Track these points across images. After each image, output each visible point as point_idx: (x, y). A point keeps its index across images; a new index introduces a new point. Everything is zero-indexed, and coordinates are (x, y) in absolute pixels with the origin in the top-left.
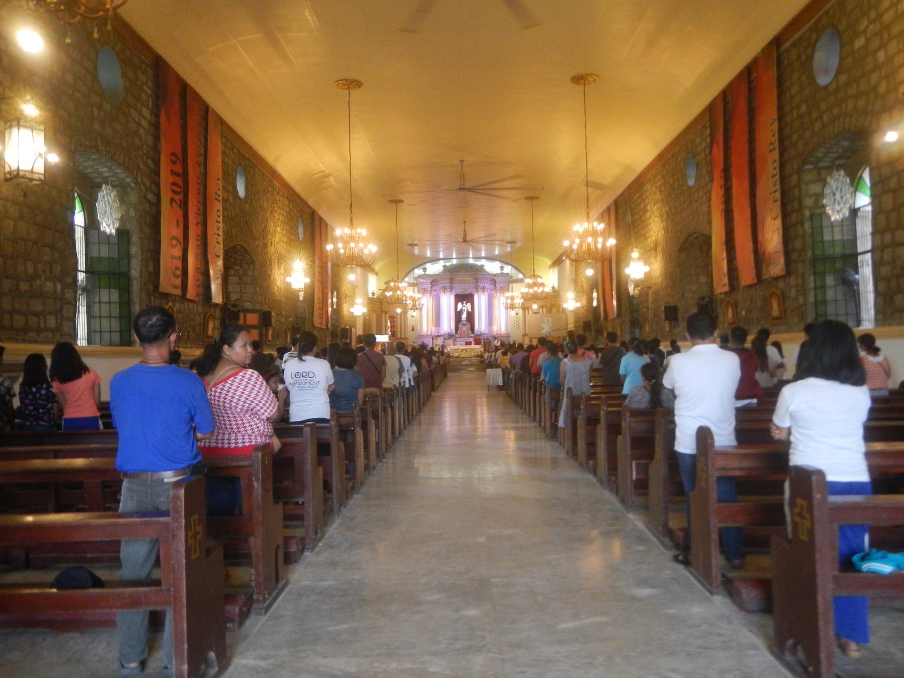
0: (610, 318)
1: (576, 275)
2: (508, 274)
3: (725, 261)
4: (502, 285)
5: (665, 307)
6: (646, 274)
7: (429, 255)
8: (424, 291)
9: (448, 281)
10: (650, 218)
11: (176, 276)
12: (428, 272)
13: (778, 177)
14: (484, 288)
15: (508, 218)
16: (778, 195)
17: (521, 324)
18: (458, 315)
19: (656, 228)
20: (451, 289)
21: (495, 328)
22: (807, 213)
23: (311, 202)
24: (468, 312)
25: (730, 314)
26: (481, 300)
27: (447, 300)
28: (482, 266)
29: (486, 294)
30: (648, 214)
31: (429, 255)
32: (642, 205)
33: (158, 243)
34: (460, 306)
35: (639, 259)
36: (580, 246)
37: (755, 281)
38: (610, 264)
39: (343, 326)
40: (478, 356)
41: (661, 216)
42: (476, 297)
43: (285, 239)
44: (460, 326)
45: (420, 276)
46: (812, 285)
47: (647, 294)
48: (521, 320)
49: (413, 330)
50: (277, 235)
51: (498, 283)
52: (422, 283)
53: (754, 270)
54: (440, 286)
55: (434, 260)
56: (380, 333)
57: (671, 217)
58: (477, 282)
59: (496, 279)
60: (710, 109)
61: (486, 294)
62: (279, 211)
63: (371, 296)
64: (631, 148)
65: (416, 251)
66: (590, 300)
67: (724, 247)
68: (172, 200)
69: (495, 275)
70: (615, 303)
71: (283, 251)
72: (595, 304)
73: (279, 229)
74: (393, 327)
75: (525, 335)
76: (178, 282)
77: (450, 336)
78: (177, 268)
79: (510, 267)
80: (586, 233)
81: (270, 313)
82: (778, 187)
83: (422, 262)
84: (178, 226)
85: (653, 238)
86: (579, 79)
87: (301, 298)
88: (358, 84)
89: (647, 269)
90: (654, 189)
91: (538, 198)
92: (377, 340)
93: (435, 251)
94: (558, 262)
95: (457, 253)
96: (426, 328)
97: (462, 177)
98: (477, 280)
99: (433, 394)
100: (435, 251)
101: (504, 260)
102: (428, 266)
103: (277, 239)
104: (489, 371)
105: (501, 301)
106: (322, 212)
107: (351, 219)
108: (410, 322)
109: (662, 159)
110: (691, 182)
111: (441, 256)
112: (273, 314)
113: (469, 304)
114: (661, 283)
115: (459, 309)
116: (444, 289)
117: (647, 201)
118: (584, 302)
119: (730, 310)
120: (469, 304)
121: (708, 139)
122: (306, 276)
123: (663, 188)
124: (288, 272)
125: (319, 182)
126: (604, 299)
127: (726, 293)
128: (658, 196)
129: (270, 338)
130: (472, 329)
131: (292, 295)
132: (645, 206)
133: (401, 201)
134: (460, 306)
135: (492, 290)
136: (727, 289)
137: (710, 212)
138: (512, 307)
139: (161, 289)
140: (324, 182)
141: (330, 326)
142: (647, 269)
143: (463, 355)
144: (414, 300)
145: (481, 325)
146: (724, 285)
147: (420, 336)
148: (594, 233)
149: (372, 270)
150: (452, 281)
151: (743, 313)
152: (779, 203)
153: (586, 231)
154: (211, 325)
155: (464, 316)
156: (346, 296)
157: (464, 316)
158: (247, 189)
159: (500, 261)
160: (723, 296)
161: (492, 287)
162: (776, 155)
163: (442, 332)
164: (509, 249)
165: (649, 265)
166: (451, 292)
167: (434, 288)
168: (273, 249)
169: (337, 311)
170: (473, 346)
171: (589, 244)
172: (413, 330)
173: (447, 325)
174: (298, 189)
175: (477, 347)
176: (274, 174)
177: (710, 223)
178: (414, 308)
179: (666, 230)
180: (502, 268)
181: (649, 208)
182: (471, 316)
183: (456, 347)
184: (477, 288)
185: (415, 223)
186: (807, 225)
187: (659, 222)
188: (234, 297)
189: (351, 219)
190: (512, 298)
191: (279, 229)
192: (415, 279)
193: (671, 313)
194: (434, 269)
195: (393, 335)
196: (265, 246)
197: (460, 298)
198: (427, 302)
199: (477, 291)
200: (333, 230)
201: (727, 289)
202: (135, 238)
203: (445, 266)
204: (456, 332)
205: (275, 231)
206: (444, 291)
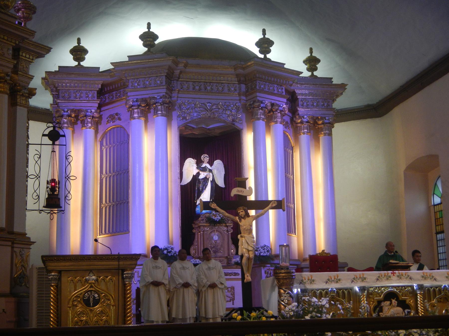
12: (88, 62)
18: (189, 192)
20: (169, 108)
24: (215, 189)
27: (153, 147)
34: (191, 168)
42: (248, 139)
54: (133, 96)
59: (301, 92)
113: (218, 164)
115: (187, 179)
116: (147, 108)
120: (218, 164)
166: (168, 116)
167: (107, 112)
173: (153, 222)
180: (312, 63)
194: (113, 43)
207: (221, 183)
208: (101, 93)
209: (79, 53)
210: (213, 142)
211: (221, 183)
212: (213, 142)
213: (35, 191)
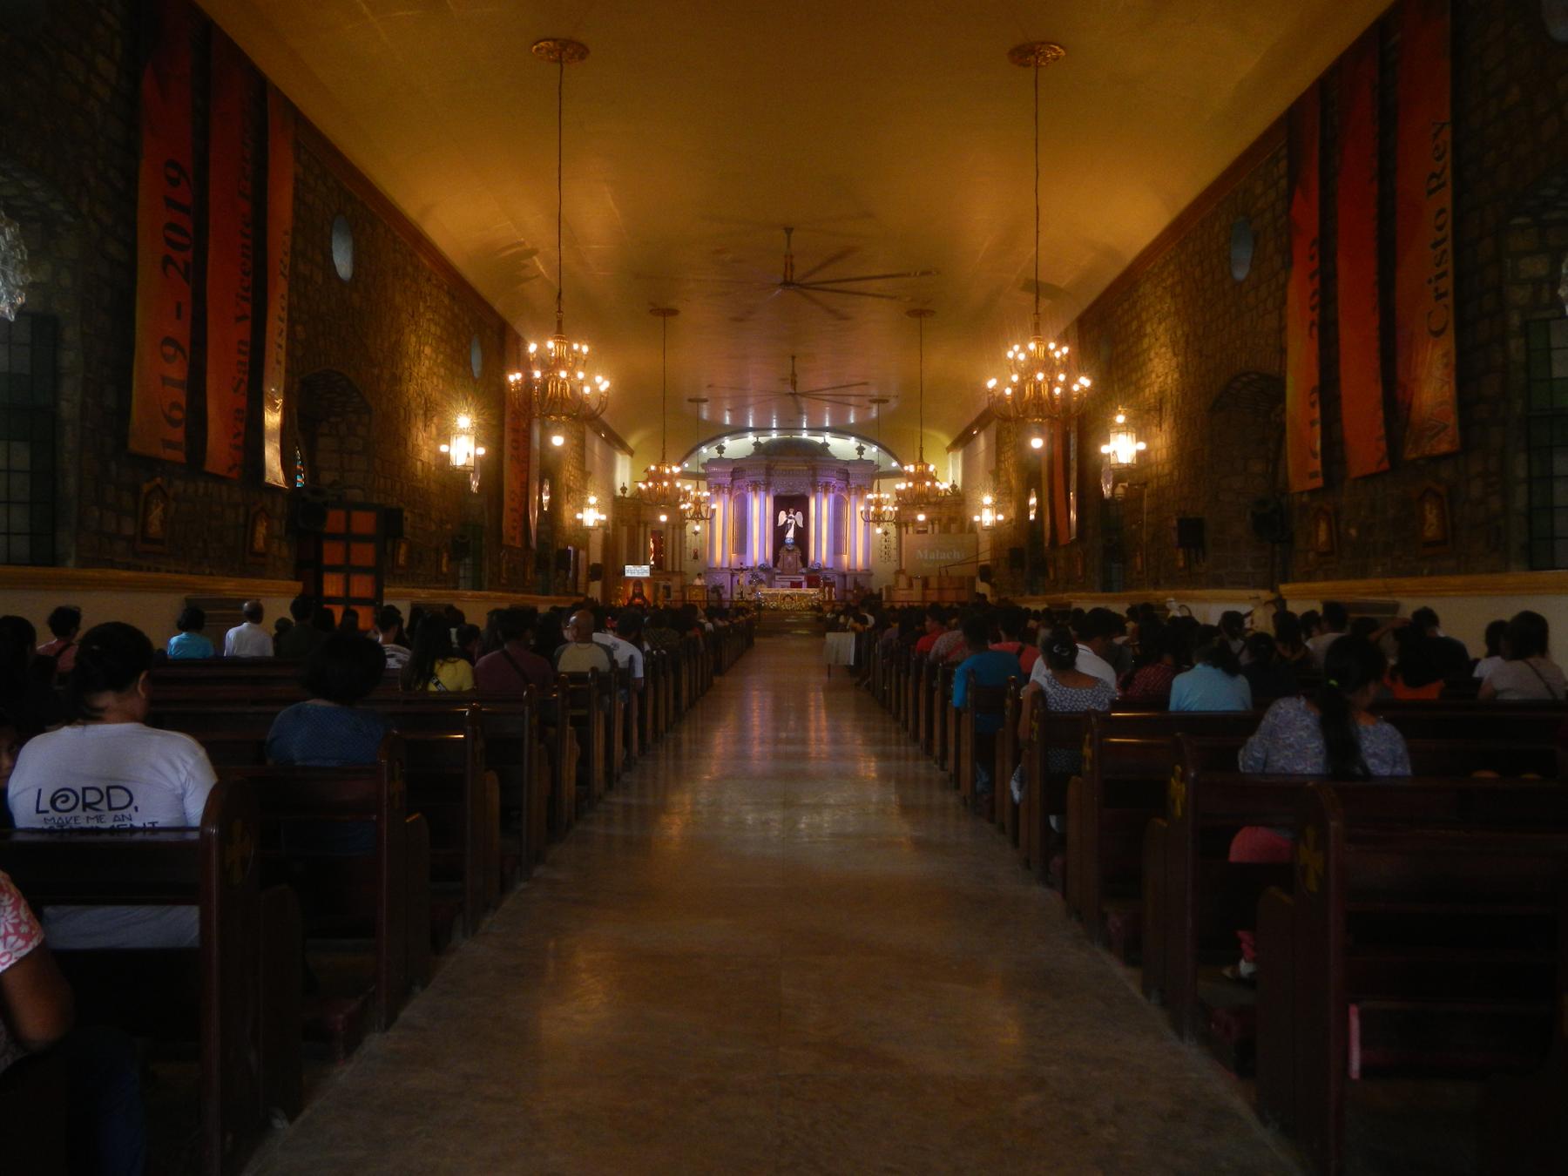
0: (1062, 541)
1: (998, 461)
2: (871, 462)
3: (1318, 428)
4: (860, 482)
5: (1180, 521)
6: (1140, 455)
7: (727, 420)
8: (717, 489)
9: (763, 471)
10: (1150, 348)
11: (174, 423)
13: (1448, 245)
14: (826, 488)
15: (876, 350)
16: (1447, 284)
17: (894, 553)
18: (779, 532)
19: (1162, 369)
20: (767, 486)
21: (845, 558)
22: (1515, 320)
23: (498, 306)
24: (797, 527)
25: (1323, 535)
26: (821, 507)
27: (759, 507)
28: (826, 445)
29: (832, 496)
30: (1146, 342)
31: (727, 420)
32: (1134, 325)
33: (129, 347)
34: (782, 517)
35: (1125, 428)
36: (1019, 390)
37: (1386, 465)
38: (1078, 427)
39: (561, 546)
40: (813, 608)
41: (1174, 344)
42: (812, 503)
43: (442, 371)
44: (782, 552)
45: (712, 462)
46: (1521, 473)
47: (1141, 497)
48: (894, 544)
49: (696, 557)
50: (424, 363)
51: (856, 477)
52: (714, 474)
53: (1383, 444)
54: (748, 479)
55: (738, 431)
56: (635, 561)
57: (1196, 347)
58: (814, 475)
59: (851, 470)
60: (1290, 121)
61: (832, 496)
62: (429, 315)
63: (619, 493)
64: (1122, 211)
65: (705, 415)
66: (1024, 509)
67: (1315, 396)
68: (167, 261)
69: (848, 463)
70: (1073, 516)
71: (436, 395)
72: (1032, 517)
73: (428, 350)
74: (658, 551)
75: (900, 572)
76: (178, 434)
77: (763, 568)
78: (174, 405)
79: (875, 449)
80: (1034, 364)
81: (400, 511)
82: (1448, 265)
83: (715, 433)
84: (178, 317)
85: (1156, 389)
86: (1026, 54)
87: (475, 484)
88: (582, 51)
89: (1142, 446)
90: (1159, 291)
91: (932, 312)
92: (628, 574)
93: (739, 411)
94: (963, 441)
95: (780, 420)
96: (721, 554)
97: (790, 267)
98: (814, 471)
99: (716, 680)
100: (739, 411)
101: (863, 433)
102: (727, 442)
103: (424, 369)
104: (830, 636)
105: (857, 510)
106: (518, 327)
107: (560, 323)
108: (691, 542)
109: (1178, 231)
110: (1240, 274)
111: (751, 425)
112: (406, 514)
114: (1171, 474)
116: (755, 486)
117: (1144, 316)
118: (1012, 513)
119: (1323, 526)
121: (1283, 183)
122: (478, 443)
123: (1178, 289)
124: (445, 435)
125: (513, 266)
126: (1052, 506)
127: (1313, 492)
128: (1168, 304)
129: (401, 560)
130: (804, 558)
131: (454, 479)
132: (1141, 326)
133: (674, 312)
134: (782, 517)
135: (842, 490)
136: (1318, 482)
137: (1281, 329)
138: (878, 519)
139: (133, 446)
140: (525, 266)
141: (533, 544)
142: (1142, 446)
143: (786, 606)
144: (697, 502)
145: (820, 551)
146: (1313, 475)
147: (710, 571)
148: (1048, 365)
149: (623, 447)
150: (769, 471)
151: (1353, 532)
152: (1449, 300)
153: (1028, 362)
154: (261, 530)
155: (790, 534)
156: (570, 490)
157: (790, 534)
158: (357, 263)
159: (858, 436)
160: (1305, 498)
161: (843, 484)
162: (1446, 198)
163: (749, 564)
164: (874, 414)
165: (1146, 439)
166: (767, 491)
167: (737, 483)
168: (412, 387)
169: (551, 517)
170: (804, 590)
171: (1038, 385)
172: (696, 557)
173: (759, 550)
174: (470, 275)
175: (811, 591)
176: (418, 240)
177: (1283, 351)
178: (697, 517)
179: (1183, 370)
180: (861, 450)
181: (1149, 330)
182: (802, 534)
183: (772, 591)
184: (814, 486)
185: (700, 356)
186: (1515, 344)
187: (1169, 355)
188: (327, 477)
189: (560, 323)
190: (879, 503)
191: (428, 350)
192: (704, 465)
193: (1192, 533)
194: (738, 447)
195: (658, 568)
196: (397, 379)
197: (782, 503)
198: (721, 508)
199: (815, 491)
200: (526, 345)
201: (1318, 482)
202: (70, 334)
203: (757, 444)
204: (775, 565)
205: (419, 353)
206: (755, 490)
207: (800, 524)
208: (733, 474)
209: (721, 449)
210: (792, 502)
211: (800, 524)
212: (792, 502)
213: (689, 553)
